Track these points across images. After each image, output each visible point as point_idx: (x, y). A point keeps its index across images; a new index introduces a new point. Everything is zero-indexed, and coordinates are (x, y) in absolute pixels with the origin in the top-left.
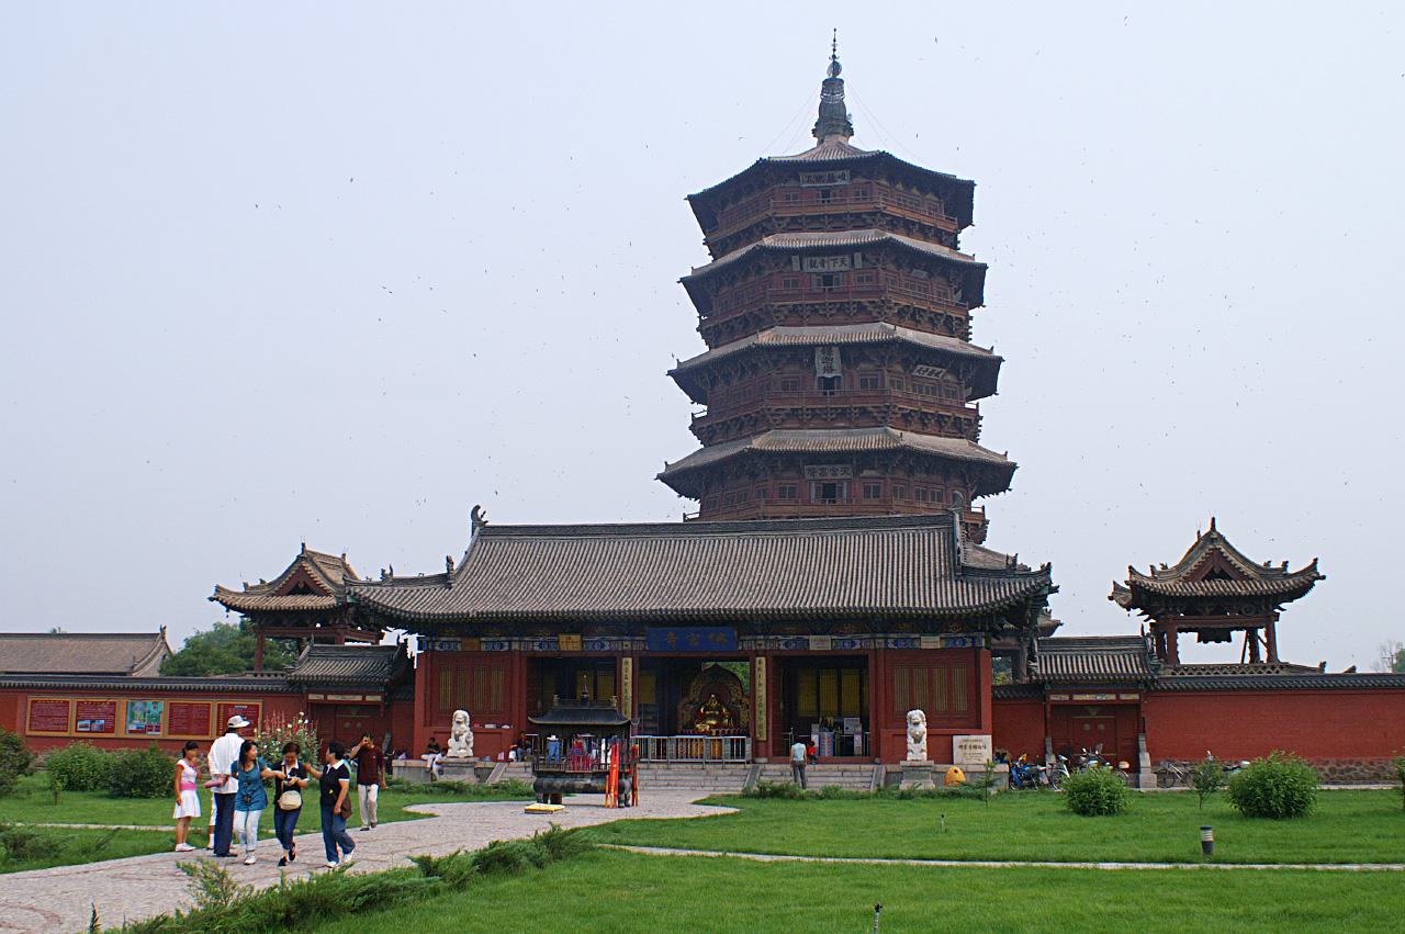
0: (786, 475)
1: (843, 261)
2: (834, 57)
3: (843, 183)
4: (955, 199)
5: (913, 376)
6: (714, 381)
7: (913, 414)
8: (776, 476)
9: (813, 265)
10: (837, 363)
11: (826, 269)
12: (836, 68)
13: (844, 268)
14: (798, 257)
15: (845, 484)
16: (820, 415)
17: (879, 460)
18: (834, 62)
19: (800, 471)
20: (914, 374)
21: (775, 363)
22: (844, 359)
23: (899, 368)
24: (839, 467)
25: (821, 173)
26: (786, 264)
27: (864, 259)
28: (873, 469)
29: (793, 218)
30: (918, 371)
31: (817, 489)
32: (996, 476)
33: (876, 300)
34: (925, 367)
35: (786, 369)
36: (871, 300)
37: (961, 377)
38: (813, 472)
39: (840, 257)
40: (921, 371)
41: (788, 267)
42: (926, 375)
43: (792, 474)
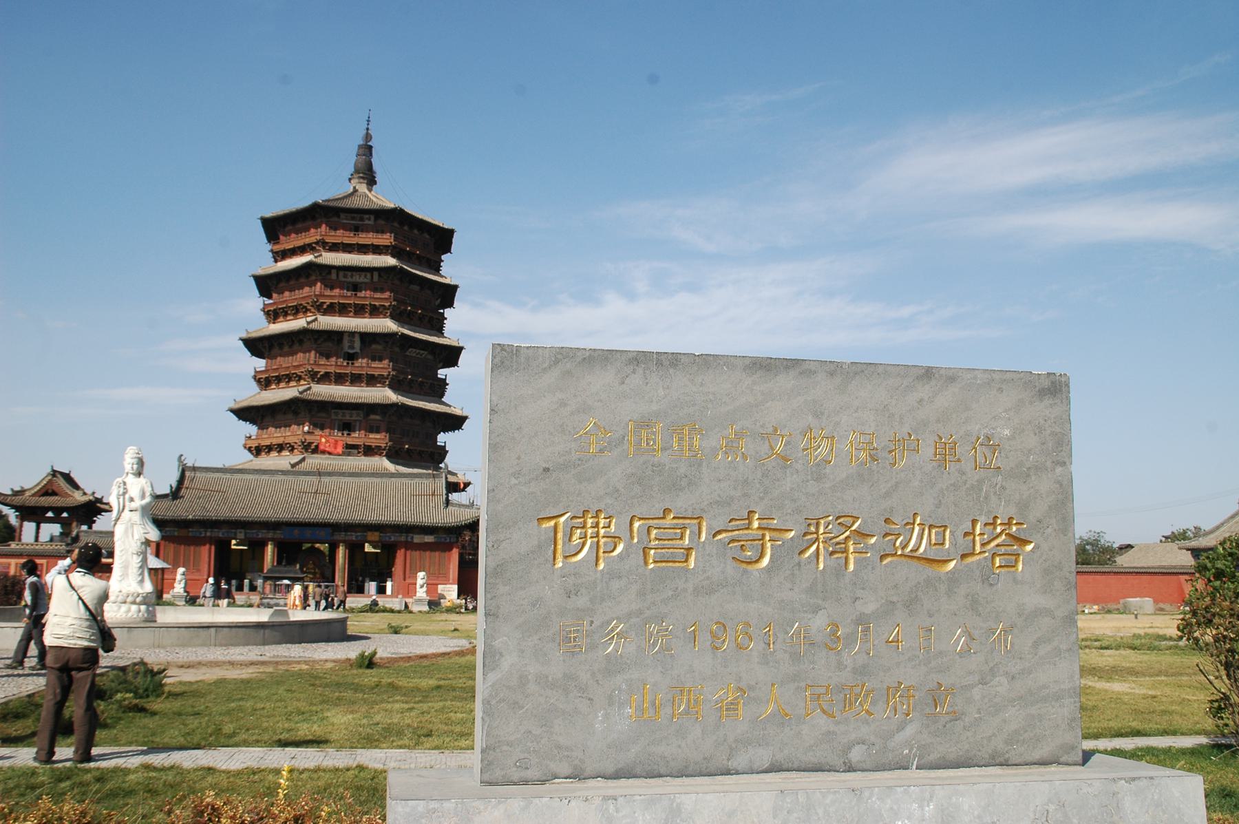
4: (441, 239)
6: (271, 347)
9: (345, 276)
10: (357, 344)
12: (368, 137)
21: (316, 340)
23: (397, 349)
29: (335, 244)
32: (455, 422)
33: (387, 304)
38: (337, 414)
40: (412, 352)
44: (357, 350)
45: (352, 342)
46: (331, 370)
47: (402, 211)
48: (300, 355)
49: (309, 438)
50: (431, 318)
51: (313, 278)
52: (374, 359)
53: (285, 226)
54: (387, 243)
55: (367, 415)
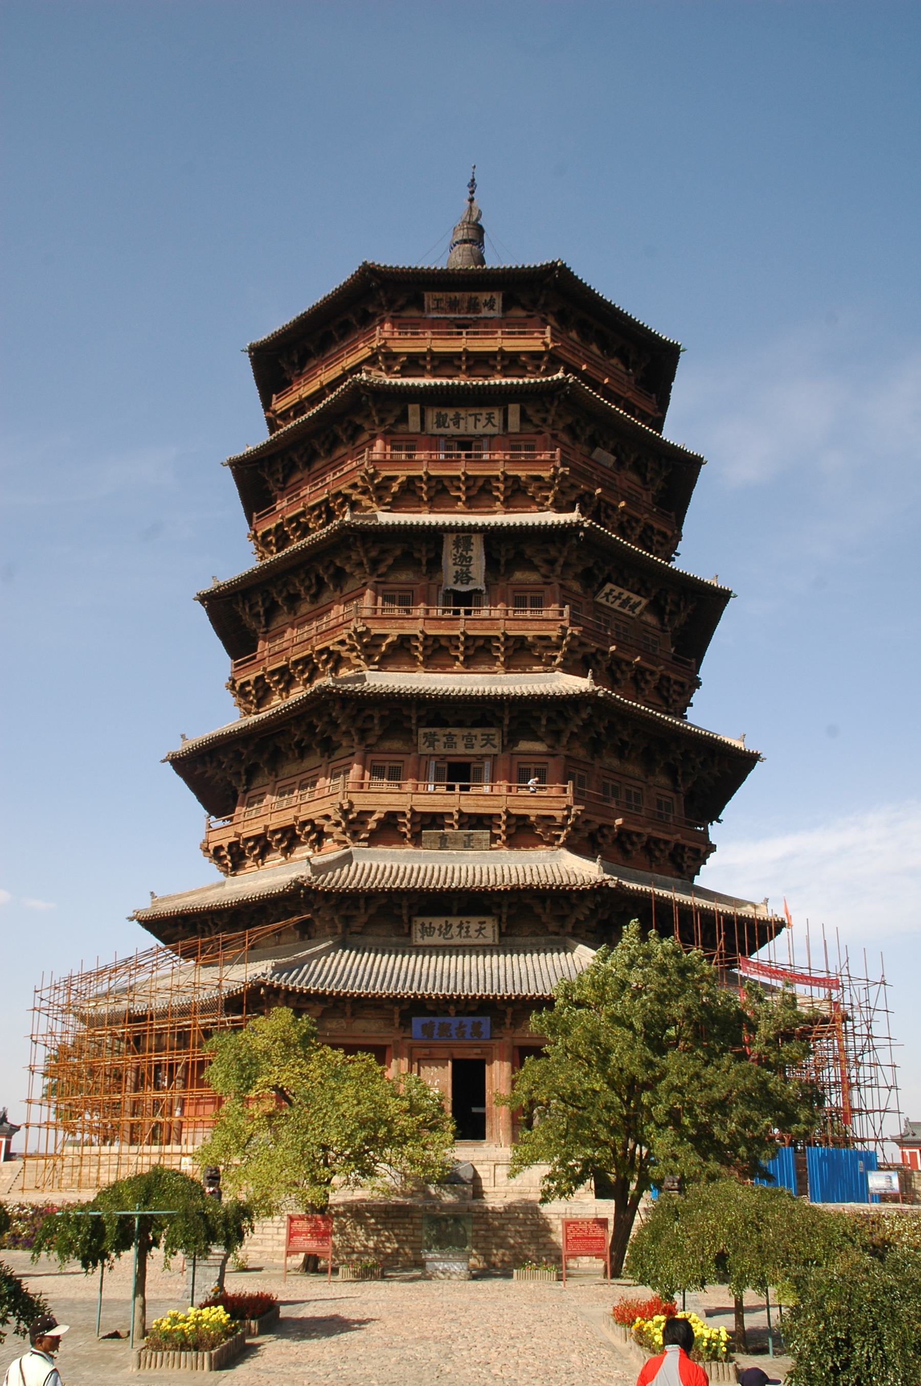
0: (387, 745)
1: (489, 419)
2: (471, 200)
3: (491, 314)
5: (597, 603)
7: (599, 658)
8: (367, 746)
9: (441, 423)
11: (461, 431)
13: (490, 430)
14: (417, 406)
15: (487, 764)
16: (447, 649)
17: (549, 720)
18: (471, 208)
19: (408, 735)
20: (598, 600)
22: (492, 564)
23: (576, 586)
24: (477, 731)
25: (458, 295)
27: (524, 418)
28: (537, 739)
29: (409, 355)
30: (607, 595)
31: (437, 769)
33: (546, 474)
34: (618, 590)
35: (391, 578)
36: (535, 473)
38: (431, 740)
39: (484, 411)
41: (401, 428)
42: (615, 606)
43: (397, 745)
45: (465, 560)
46: (414, 628)
47: (564, 271)
48: (338, 611)
49: (361, 802)
50: (648, 527)
51: (365, 437)
52: (519, 602)
53: (302, 364)
55: (511, 740)
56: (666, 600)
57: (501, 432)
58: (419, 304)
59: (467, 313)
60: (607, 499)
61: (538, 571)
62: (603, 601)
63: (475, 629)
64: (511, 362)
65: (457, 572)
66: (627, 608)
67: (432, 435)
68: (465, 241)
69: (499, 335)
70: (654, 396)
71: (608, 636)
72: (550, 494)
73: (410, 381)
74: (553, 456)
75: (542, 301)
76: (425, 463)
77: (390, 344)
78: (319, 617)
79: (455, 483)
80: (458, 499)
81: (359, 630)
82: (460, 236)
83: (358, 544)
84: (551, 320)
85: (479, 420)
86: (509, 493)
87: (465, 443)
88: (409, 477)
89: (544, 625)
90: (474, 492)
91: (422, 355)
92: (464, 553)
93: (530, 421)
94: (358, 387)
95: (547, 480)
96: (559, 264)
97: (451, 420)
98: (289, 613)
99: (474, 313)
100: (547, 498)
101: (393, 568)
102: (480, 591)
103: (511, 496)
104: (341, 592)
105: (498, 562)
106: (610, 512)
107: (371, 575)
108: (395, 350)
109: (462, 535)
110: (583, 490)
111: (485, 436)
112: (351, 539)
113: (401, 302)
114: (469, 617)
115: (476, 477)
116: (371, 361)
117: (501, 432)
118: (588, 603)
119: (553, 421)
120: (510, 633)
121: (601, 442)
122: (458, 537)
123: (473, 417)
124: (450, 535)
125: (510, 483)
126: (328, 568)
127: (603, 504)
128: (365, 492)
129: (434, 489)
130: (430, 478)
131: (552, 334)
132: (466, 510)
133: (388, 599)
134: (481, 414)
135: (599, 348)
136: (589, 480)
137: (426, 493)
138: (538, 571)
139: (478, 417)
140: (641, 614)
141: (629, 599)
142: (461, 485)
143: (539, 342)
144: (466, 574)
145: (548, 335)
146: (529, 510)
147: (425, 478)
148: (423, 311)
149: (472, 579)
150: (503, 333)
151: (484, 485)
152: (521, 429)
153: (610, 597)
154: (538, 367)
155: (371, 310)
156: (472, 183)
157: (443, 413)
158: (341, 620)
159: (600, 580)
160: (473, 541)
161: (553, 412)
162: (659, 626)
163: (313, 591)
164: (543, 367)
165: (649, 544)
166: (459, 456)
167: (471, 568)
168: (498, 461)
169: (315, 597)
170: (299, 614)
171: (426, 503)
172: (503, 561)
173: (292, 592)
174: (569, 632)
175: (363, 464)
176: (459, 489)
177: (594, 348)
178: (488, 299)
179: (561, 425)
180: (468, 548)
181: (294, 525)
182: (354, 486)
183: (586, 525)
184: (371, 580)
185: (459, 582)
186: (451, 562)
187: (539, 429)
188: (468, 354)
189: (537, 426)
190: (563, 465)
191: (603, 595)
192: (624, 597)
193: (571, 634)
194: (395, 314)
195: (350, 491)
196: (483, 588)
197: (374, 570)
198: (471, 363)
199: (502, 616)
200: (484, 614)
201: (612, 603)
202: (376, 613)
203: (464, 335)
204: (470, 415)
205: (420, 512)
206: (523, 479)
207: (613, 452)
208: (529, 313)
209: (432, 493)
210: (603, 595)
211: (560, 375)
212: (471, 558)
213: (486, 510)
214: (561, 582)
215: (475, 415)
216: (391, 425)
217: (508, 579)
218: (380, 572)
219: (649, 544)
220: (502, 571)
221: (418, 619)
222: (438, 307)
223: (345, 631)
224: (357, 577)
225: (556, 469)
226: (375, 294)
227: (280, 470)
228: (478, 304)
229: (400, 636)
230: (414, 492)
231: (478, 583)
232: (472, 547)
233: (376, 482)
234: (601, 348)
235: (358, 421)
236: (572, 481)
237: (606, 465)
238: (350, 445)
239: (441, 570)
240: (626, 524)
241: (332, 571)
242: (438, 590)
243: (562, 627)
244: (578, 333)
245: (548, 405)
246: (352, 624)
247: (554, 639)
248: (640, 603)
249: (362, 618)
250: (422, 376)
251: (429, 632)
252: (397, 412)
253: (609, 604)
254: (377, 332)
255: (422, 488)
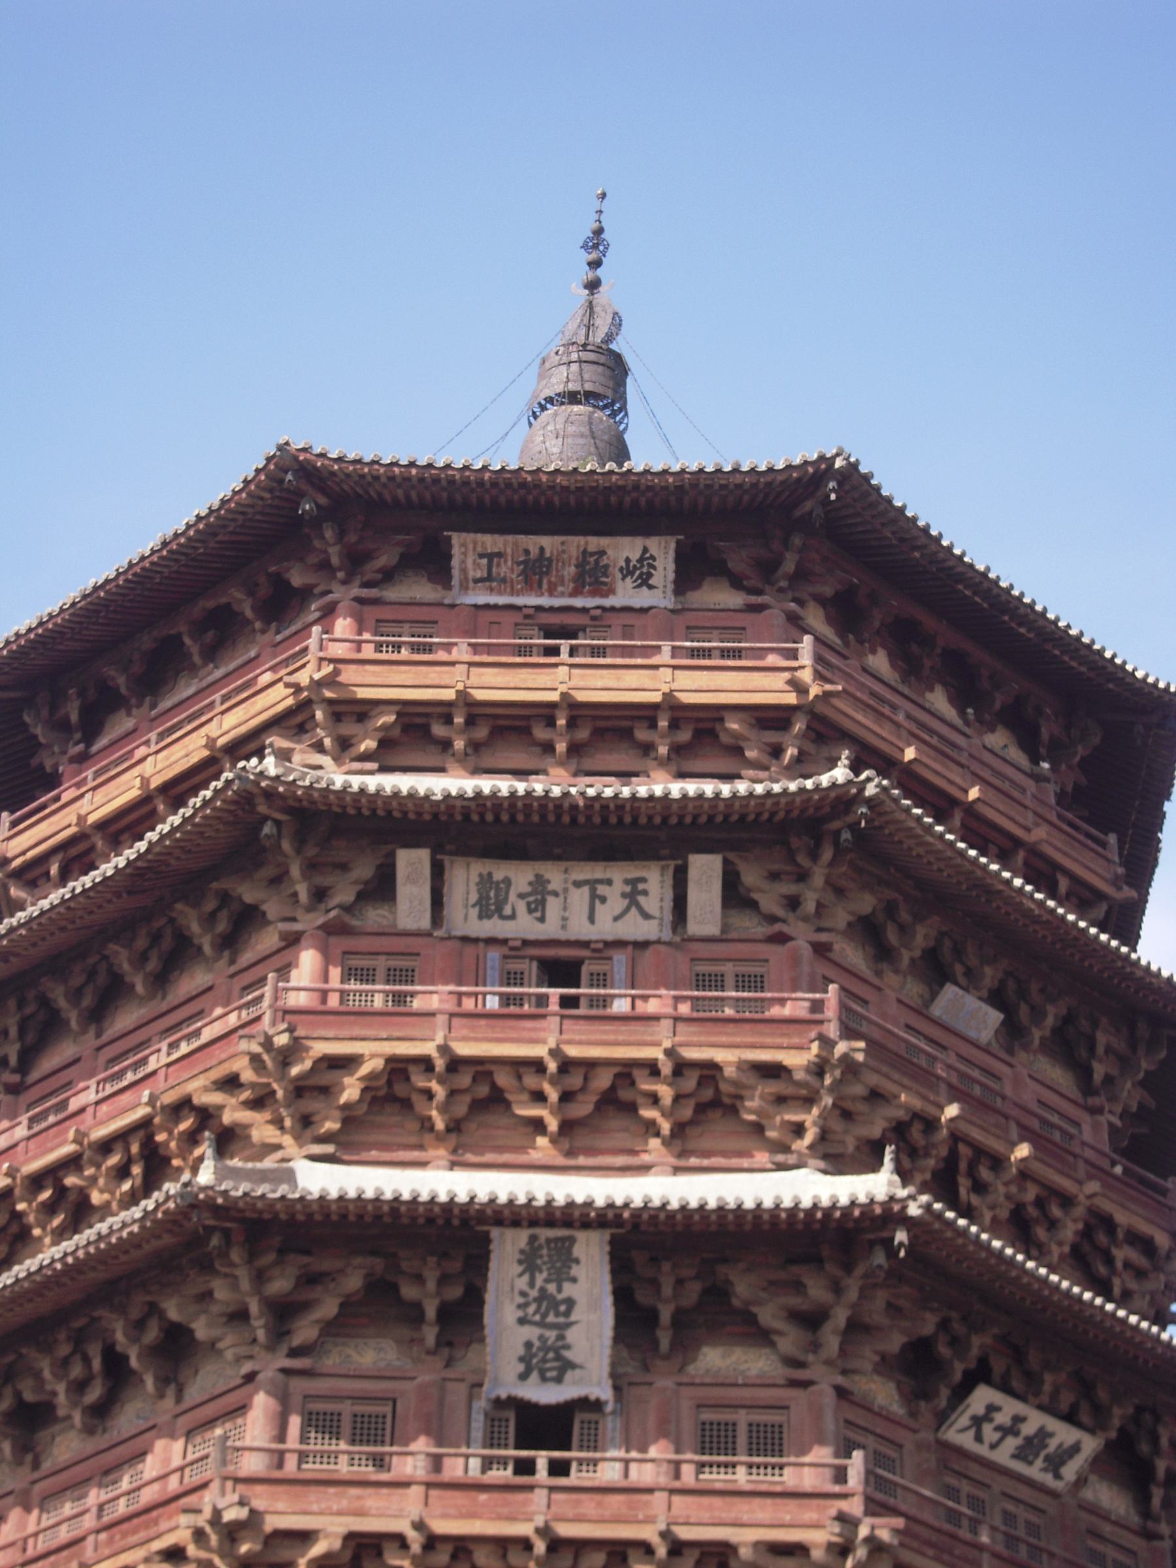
1: (633, 895)
2: (593, 286)
3: (643, 598)
9: (491, 903)
11: (550, 929)
13: (635, 928)
14: (423, 856)
18: (591, 306)
22: (633, 1320)
23: (884, 1393)
26: (362, 897)
27: (734, 895)
29: (405, 709)
30: (977, 1422)
34: (1010, 1407)
35: (331, 1361)
37: (1157, 1496)
39: (619, 874)
41: (375, 916)
42: (1003, 1455)
44: (592, 1378)
45: (552, 1309)
48: (166, 1454)
50: (1101, 1222)
51: (267, 940)
52: (715, 1441)
53: (91, 728)
54: (770, 689)
56: (1155, 1440)
57: (667, 935)
58: (433, 562)
59: (575, 593)
60: (976, 1134)
61: (772, 1344)
62: (966, 1440)
63: (579, 1519)
64: (700, 733)
65: (528, 1345)
66: (1039, 1463)
67: (465, 939)
68: (573, 398)
69: (665, 657)
70: (1112, 839)
71: (980, 1548)
72: (810, 1118)
73: (403, 783)
74: (817, 1006)
75: (789, 565)
76: (441, 1019)
77: (349, 675)
78: (108, 1473)
79: (530, 1081)
80: (538, 1125)
81: (229, 1516)
82: (557, 382)
83: (235, 1255)
84: (815, 617)
85: (603, 900)
86: (687, 1112)
87: (561, 968)
88: (391, 1060)
89: (789, 1511)
90: (582, 1108)
91: (443, 711)
92: (552, 1288)
93: (753, 905)
94: (251, 801)
95: (799, 1076)
96: (839, 463)
97: (521, 896)
98: (19, 1462)
99: (594, 593)
100: (799, 1130)
101: (335, 1329)
102: (596, 1406)
103: (692, 1122)
104: (179, 1398)
105: (650, 1318)
106: (985, 1173)
107: (271, 1347)
108: (363, 693)
109: (545, 1233)
110: (906, 1107)
111: (619, 944)
112: (215, 1241)
113: (386, 559)
114: (562, 1481)
115: (590, 1065)
116: (294, 721)
117: (667, 935)
118: (919, 1446)
119: (820, 906)
120: (685, 1533)
121: (959, 969)
122: (533, 1239)
123: (586, 890)
124: (510, 1233)
125: (690, 1083)
126: (140, 1325)
127: (963, 1149)
128: (257, 1103)
129: (467, 1099)
130: (456, 1064)
131: (818, 659)
132: (561, 1161)
133: (321, 1422)
134: (609, 882)
135: (952, 701)
136: (923, 1077)
137: (444, 1109)
138: (772, 1344)
139: (601, 890)
140: (1081, 1481)
141: (1043, 1435)
142: (547, 1088)
143: (779, 681)
144: (557, 1350)
145: (806, 658)
146: (745, 1162)
147: (440, 1064)
148: (447, 586)
149: (571, 1365)
150: (675, 652)
151: (613, 1088)
152: (725, 928)
153: (987, 1429)
154: (776, 751)
155: (297, 578)
156: (597, 240)
157: (498, 875)
158: (173, 1484)
159: (958, 1376)
160: (578, 1251)
161: (818, 879)
162: (1135, 1519)
163: (94, 1393)
164: (791, 752)
165: (1102, 1270)
166: (542, 1000)
167: (572, 1335)
168: (656, 1018)
169: (101, 1412)
170: (47, 1465)
171: (440, 1138)
172: (666, 1314)
173: (29, 1397)
174: (863, 1531)
175: (258, 1018)
176: (539, 1097)
177: (939, 700)
178: (635, 556)
179: (841, 917)
180: (562, 1275)
181: (46, 1195)
182: (231, 1083)
183: (914, 1210)
184: (271, 1365)
185: (535, 1375)
186: (510, 1314)
187: (778, 927)
188: (578, 712)
189: (772, 919)
190: (849, 1033)
191: (964, 1421)
192: (1028, 1429)
193: (870, 1540)
194: (366, 593)
195: (215, 1098)
196: (605, 1393)
197: (279, 1332)
198: (583, 734)
199: (663, 1480)
200: (609, 1473)
201: (993, 1446)
202: (280, 1465)
203: (564, 656)
204: (578, 884)
205: (422, 1164)
206: (729, 1072)
207: (996, 999)
208: (754, 599)
209: (461, 1109)
210: (964, 1421)
211: (840, 773)
212: (570, 1303)
213: (620, 1160)
214: (840, 1380)
215: (592, 884)
216: (347, 909)
217: (681, 1369)
218: (297, 1340)
219: (1102, 1270)
220: (665, 1340)
221: (406, 1484)
222: (489, 578)
223: (184, 1520)
224: (229, 1355)
225: (827, 1043)
226: (310, 534)
227: (13, 1032)
228: (605, 570)
229: (351, 1537)
230: (406, 1104)
231: (592, 1378)
232: (575, 1271)
233: (295, 1071)
234: (960, 700)
235: (249, 894)
236: (873, 1079)
237: (972, 1034)
238: (222, 962)
239: (482, 1340)
240: (1032, 1211)
241: (152, 1334)
242: (470, 1398)
243: (841, 1518)
244: (892, 657)
245: (803, 860)
246: (208, 1500)
247: (817, 1554)
248: (1076, 1449)
249: (237, 1480)
250: (441, 770)
251: (441, 1527)
252: (364, 870)
253: (982, 1450)
254: (312, 642)
255: (429, 1095)
